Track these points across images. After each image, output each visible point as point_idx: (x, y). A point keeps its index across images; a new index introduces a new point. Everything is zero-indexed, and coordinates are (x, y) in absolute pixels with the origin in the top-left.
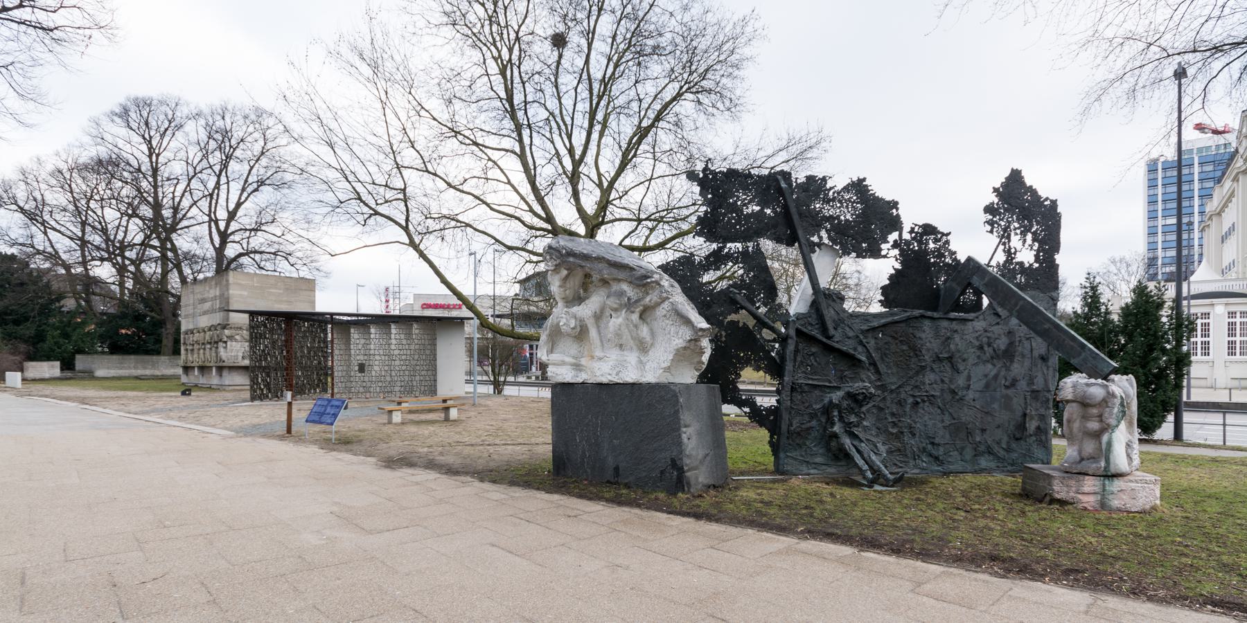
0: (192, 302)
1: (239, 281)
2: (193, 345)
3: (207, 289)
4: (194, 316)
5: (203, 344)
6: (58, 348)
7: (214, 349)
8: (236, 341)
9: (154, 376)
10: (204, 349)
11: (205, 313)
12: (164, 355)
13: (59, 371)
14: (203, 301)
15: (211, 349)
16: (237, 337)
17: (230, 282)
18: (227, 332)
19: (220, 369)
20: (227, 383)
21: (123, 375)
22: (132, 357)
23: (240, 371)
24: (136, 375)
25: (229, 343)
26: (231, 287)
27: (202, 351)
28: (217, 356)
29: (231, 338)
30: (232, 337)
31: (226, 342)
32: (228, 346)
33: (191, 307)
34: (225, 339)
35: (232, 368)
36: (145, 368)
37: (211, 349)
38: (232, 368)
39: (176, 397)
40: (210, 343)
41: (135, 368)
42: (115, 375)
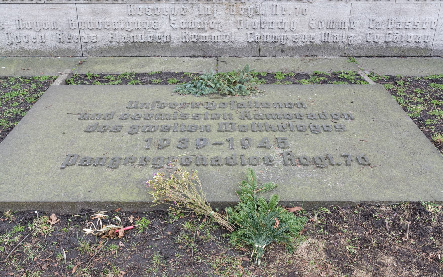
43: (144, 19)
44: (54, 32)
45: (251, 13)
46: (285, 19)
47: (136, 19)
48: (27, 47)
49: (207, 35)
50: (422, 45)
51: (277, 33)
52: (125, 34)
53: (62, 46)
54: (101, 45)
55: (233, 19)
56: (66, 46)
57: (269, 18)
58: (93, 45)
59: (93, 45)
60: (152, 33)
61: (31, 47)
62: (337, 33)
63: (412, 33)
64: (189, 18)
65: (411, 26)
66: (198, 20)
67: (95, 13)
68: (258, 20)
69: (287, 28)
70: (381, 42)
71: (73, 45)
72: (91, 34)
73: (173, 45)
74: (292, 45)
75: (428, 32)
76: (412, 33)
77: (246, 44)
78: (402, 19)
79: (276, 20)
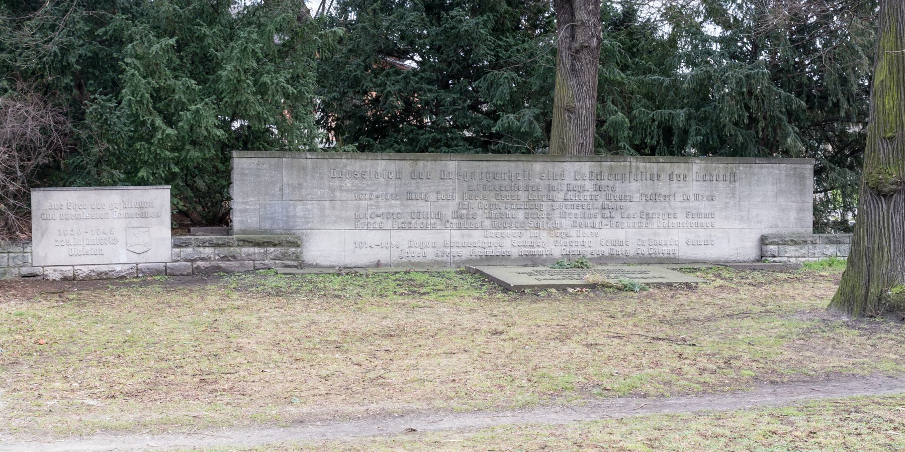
6: (170, 123)
12: (563, 154)
13: (168, 232)
21: (416, 254)
22: (452, 164)
24: (465, 253)
36: (500, 222)
41: (464, 220)
42: (382, 255)
43: (495, 240)
44: (433, 249)
45: (564, 236)
46: (586, 239)
47: (490, 240)
48: (412, 260)
49: (536, 250)
50: (672, 256)
51: (580, 249)
52: (481, 250)
53: (437, 259)
54: (464, 258)
55: (552, 240)
56: (440, 259)
57: (575, 239)
58: (458, 258)
59: (458, 258)
60: (499, 249)
61: (416, 260)
62: (618, 248)
63: (665, 248)
64: (523, 239)
65: (663, 243)
66: (530, 240)
67: (463, 236)
68: (568, 240)
69: (587, 245)
70: (646, 254)
71: (445, 258)
72: (459, 250)
73: (512, 257)
74: (590, 256)
75: (674, 247)
76: (665, 248)
77: (561, 256)
78: (657, 239)
79: (579, 240)
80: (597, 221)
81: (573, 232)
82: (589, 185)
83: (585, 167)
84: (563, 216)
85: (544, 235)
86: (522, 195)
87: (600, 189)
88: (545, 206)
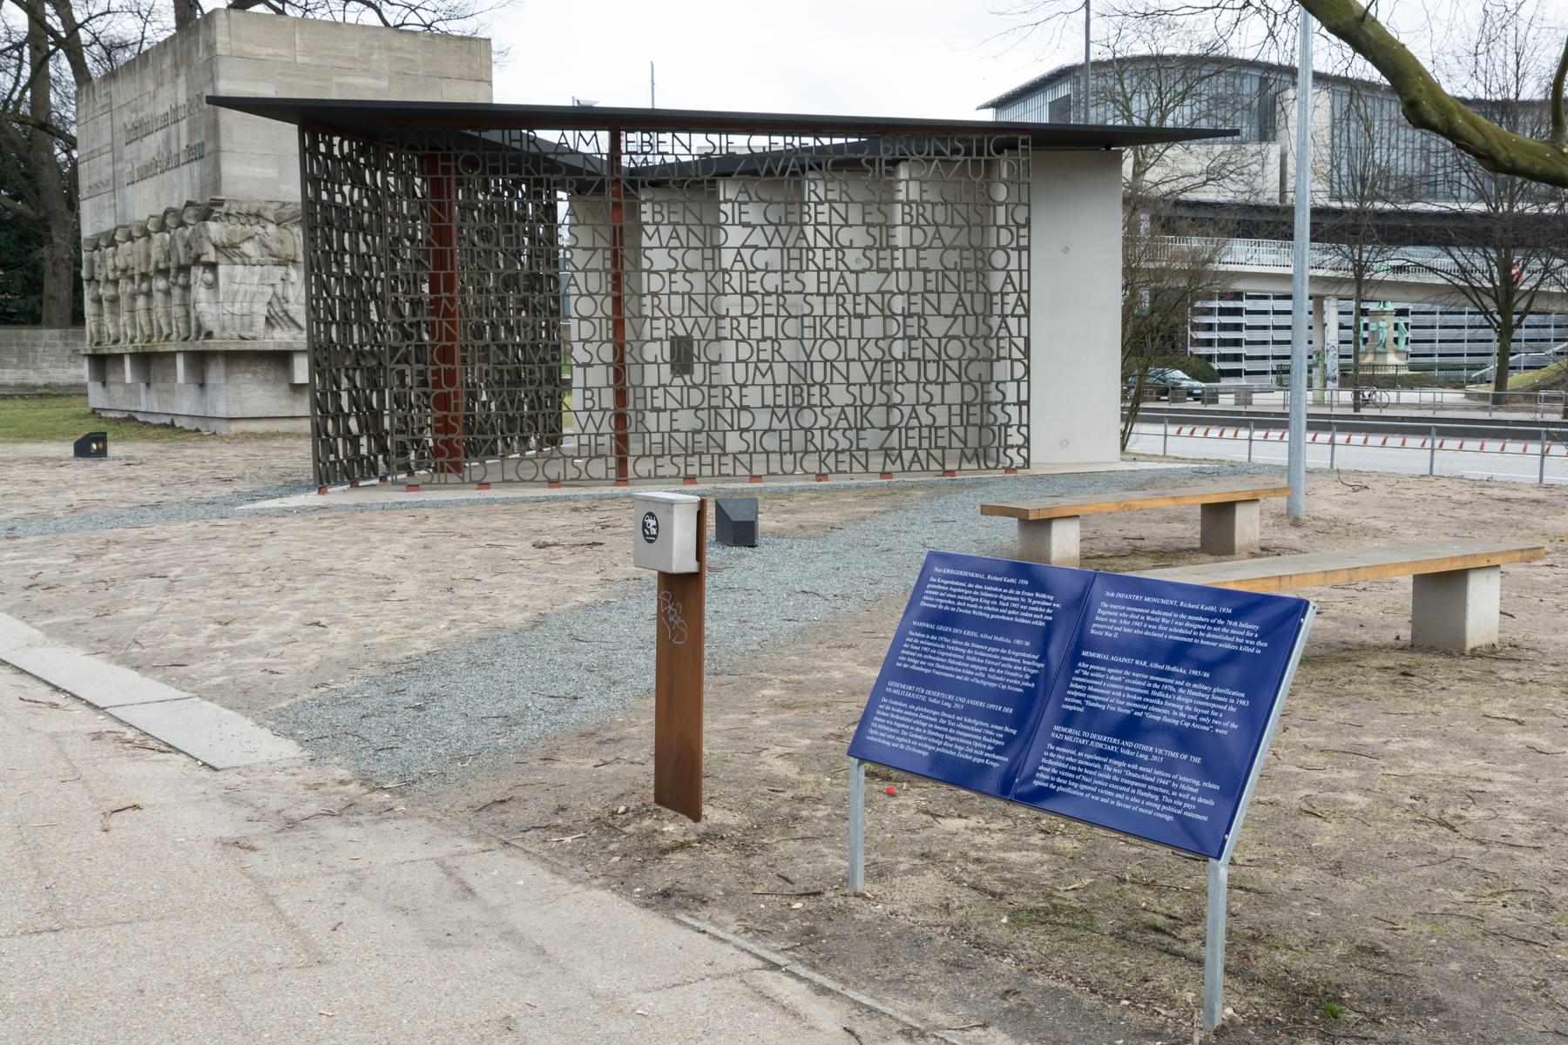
0: (107, 139)
1: (249, 48)
2: (116, 282)
3: (151, 87)
4: (114, 185)
5: (145, 276)
7: (176, 292)
8: (246, 261)
9: (23, 386)
10: (149, 294)
11: (146, 173)
12: (50, 325)
14: (139, 131)
15: (167, 293)
16: (249, 248)
17: (221, 49)
18: (215, 229)
19: (200, 360)
20: (222, 411)
23: (261, 368)
25: (222, 269)
26: (223, 68)
27: (141, 302)
28: (188, 315)
29: (228, 249)
30: (234, 246)
31: (212, 266)
32: (222, 280)
33: (107, 157)
34: (211, 256)
35: (237, 358)
37: (167, 293)
38: (237, 358)
39: (58, 462)
40: (164, 273)
80: (66, 364)
81: (51, 371)
82: (59, 343)
83: (56, 332)
84: (43, 361)
85: (31, 373)
86: (15, 349)
87: (67, 345)
88: (31, 355)
